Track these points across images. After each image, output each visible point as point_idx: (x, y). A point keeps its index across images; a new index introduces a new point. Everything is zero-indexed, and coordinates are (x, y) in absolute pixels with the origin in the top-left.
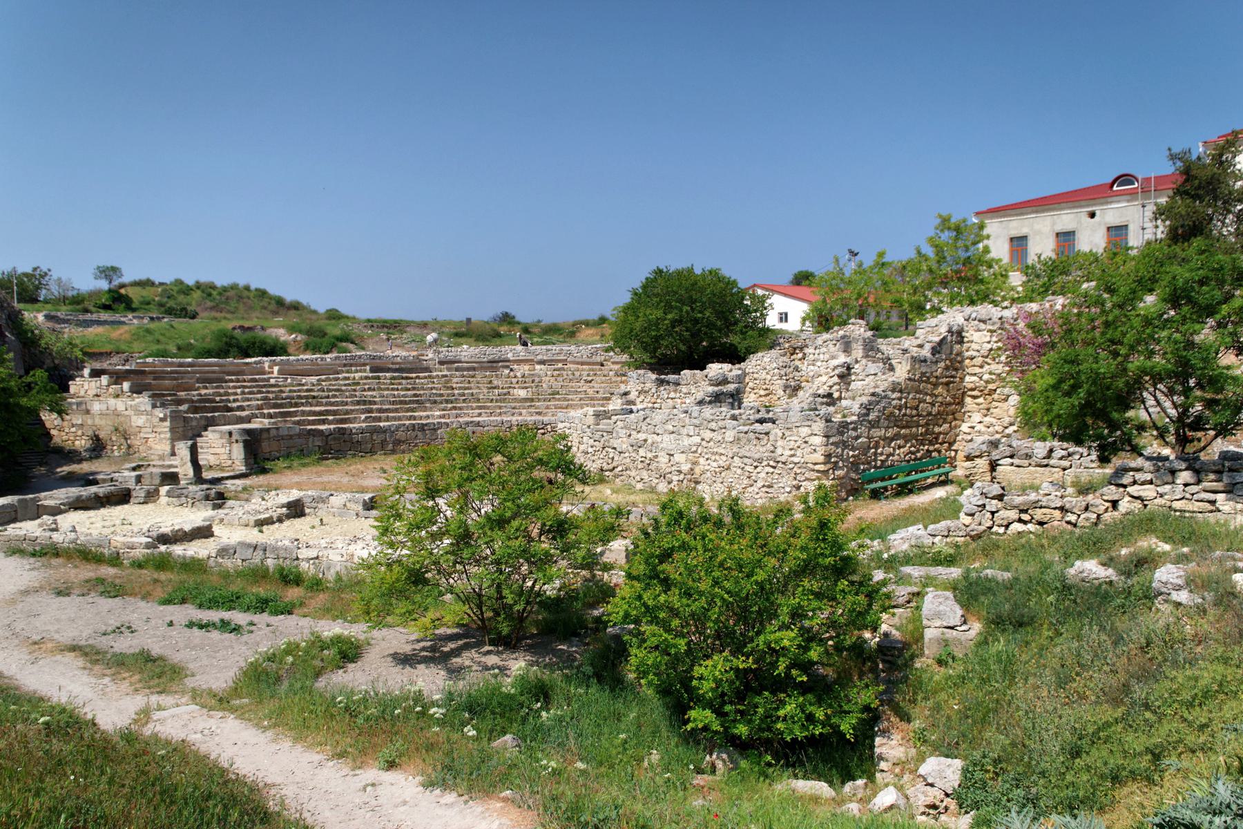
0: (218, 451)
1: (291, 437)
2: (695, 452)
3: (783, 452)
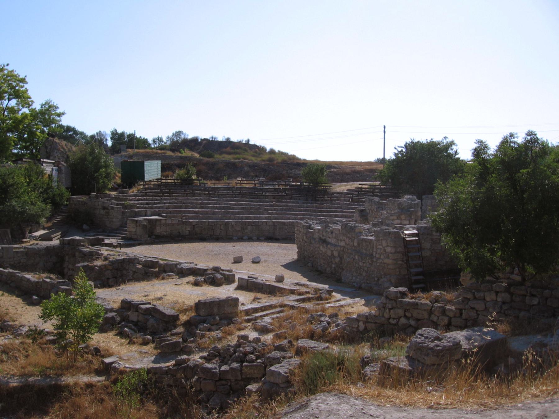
1: (173, 224)
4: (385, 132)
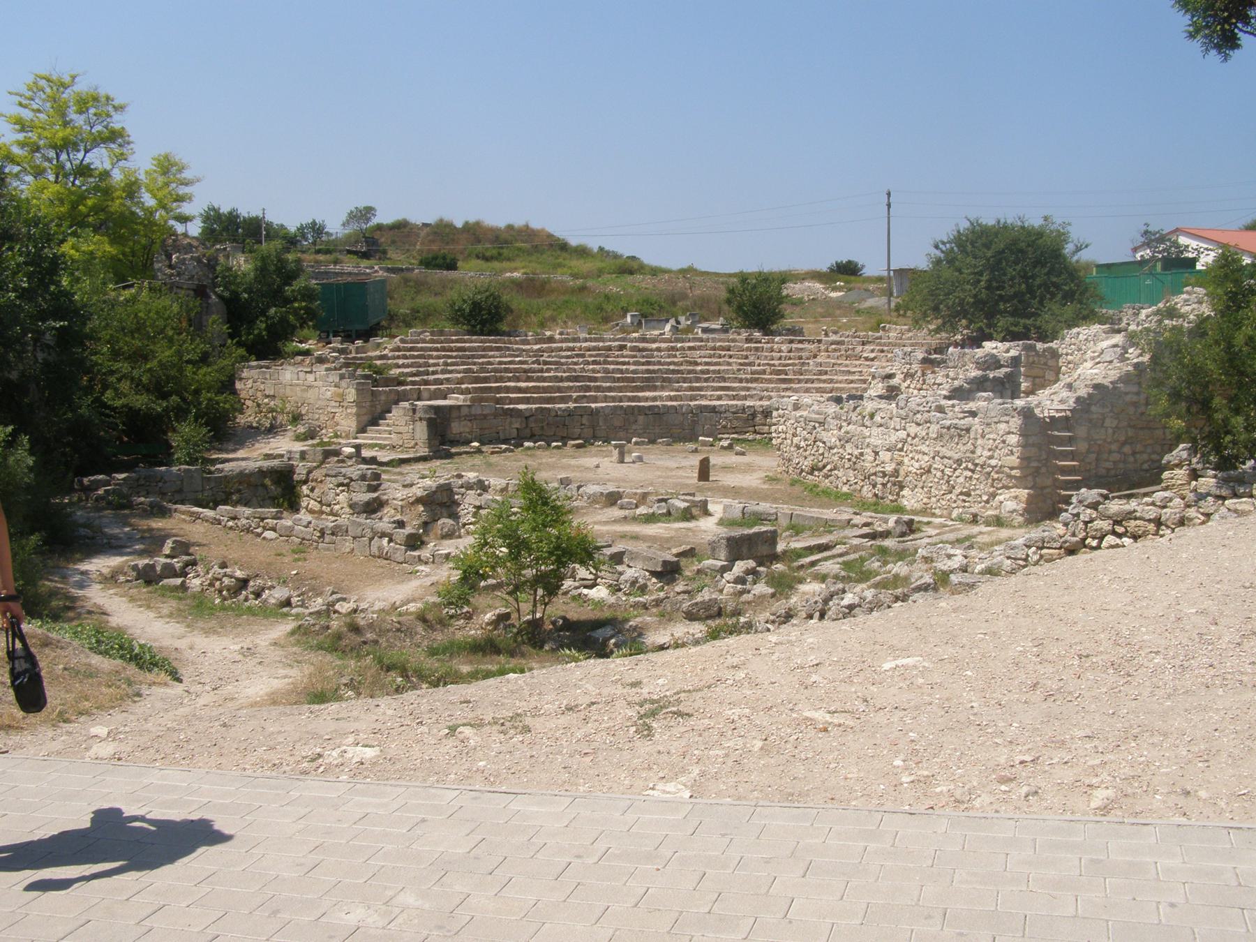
0: (401, 429)
1: (485, 416)
2: (901, 450)
3: (982, 454)
4: (889, 205)
